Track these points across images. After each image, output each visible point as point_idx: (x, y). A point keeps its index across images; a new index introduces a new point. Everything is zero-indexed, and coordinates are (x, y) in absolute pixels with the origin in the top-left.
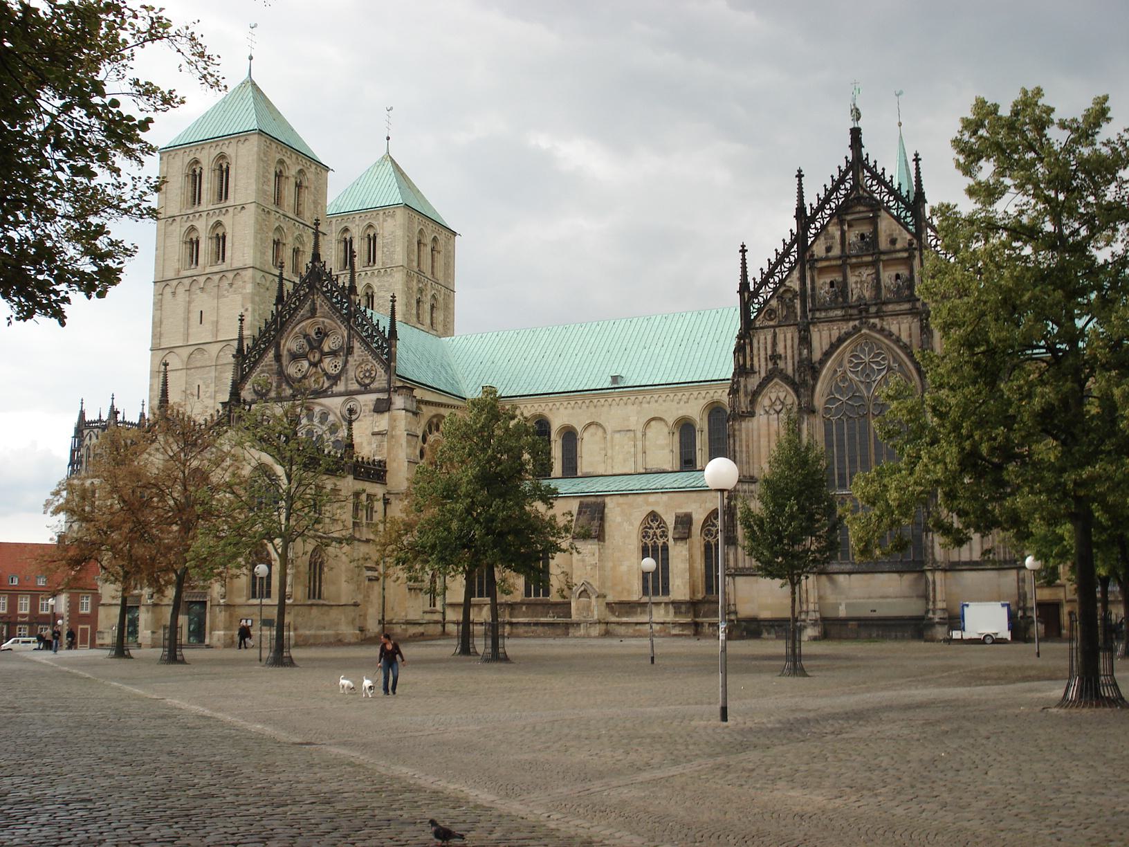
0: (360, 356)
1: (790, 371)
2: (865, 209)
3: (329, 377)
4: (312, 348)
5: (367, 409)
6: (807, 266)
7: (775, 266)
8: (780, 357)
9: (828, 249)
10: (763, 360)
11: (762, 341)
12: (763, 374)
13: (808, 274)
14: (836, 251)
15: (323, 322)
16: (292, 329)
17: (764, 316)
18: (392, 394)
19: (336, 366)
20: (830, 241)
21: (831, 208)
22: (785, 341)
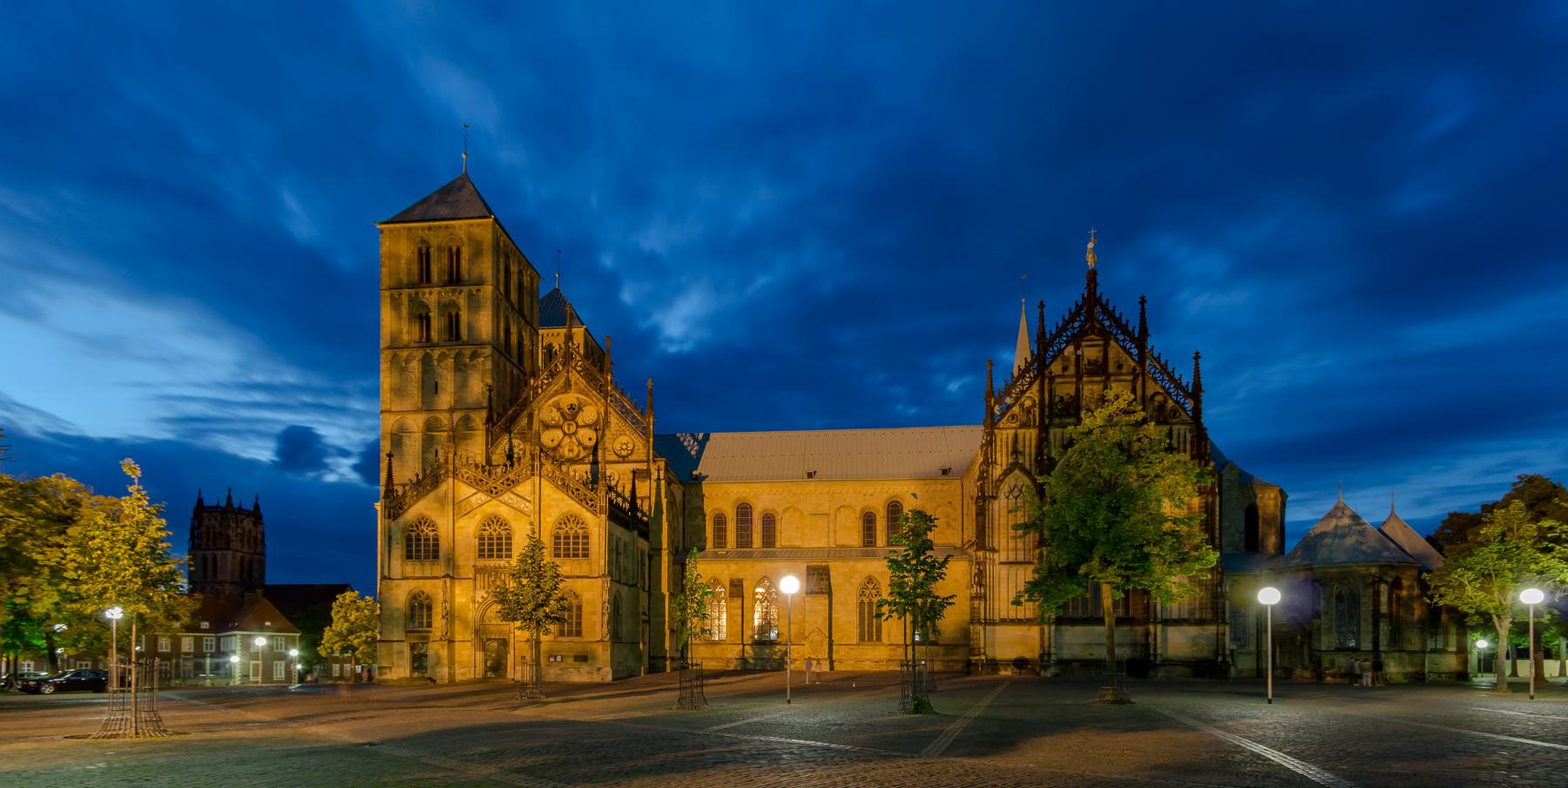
0: (617, 431)
1: (1027, 466)
2: (1097, 338)
3: (585, 448)
4: (565, 420)
5: (626, 477)
6: (1047, 381)
7: (1018, 380)
8: (1021, 453)
9: (1065, 369)
10: (1004, 455)
11: (1004, 440)
12: (1004, 467)
13: (1046, 387)
14: (1072, 370)
15: (578, 399)
16: (546, 401)
17: (1008, 420)
18: (651, 464)
19: (590, 439)
20: (1066, 362)
21: (1067, 336)
22: (1024, 441)
